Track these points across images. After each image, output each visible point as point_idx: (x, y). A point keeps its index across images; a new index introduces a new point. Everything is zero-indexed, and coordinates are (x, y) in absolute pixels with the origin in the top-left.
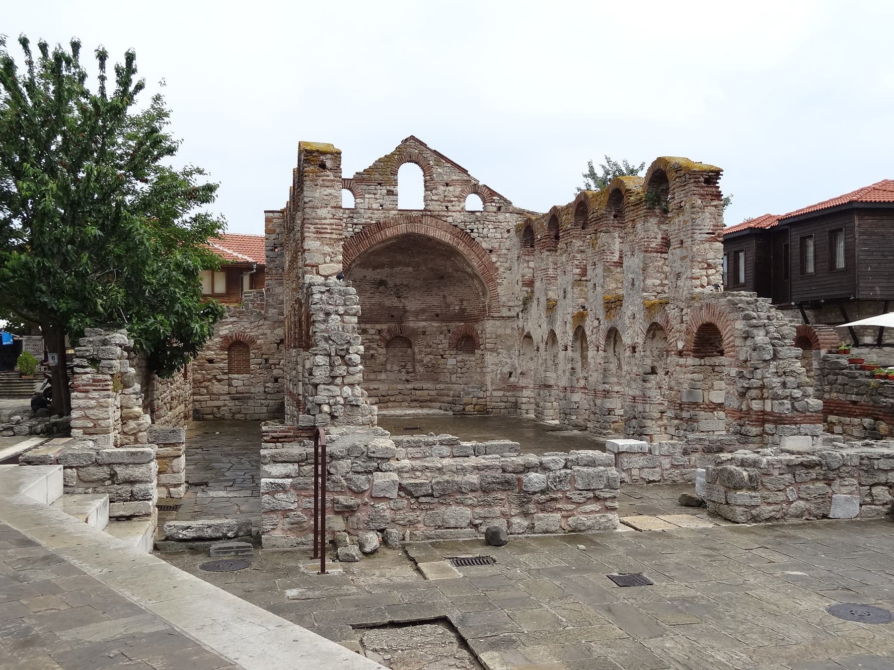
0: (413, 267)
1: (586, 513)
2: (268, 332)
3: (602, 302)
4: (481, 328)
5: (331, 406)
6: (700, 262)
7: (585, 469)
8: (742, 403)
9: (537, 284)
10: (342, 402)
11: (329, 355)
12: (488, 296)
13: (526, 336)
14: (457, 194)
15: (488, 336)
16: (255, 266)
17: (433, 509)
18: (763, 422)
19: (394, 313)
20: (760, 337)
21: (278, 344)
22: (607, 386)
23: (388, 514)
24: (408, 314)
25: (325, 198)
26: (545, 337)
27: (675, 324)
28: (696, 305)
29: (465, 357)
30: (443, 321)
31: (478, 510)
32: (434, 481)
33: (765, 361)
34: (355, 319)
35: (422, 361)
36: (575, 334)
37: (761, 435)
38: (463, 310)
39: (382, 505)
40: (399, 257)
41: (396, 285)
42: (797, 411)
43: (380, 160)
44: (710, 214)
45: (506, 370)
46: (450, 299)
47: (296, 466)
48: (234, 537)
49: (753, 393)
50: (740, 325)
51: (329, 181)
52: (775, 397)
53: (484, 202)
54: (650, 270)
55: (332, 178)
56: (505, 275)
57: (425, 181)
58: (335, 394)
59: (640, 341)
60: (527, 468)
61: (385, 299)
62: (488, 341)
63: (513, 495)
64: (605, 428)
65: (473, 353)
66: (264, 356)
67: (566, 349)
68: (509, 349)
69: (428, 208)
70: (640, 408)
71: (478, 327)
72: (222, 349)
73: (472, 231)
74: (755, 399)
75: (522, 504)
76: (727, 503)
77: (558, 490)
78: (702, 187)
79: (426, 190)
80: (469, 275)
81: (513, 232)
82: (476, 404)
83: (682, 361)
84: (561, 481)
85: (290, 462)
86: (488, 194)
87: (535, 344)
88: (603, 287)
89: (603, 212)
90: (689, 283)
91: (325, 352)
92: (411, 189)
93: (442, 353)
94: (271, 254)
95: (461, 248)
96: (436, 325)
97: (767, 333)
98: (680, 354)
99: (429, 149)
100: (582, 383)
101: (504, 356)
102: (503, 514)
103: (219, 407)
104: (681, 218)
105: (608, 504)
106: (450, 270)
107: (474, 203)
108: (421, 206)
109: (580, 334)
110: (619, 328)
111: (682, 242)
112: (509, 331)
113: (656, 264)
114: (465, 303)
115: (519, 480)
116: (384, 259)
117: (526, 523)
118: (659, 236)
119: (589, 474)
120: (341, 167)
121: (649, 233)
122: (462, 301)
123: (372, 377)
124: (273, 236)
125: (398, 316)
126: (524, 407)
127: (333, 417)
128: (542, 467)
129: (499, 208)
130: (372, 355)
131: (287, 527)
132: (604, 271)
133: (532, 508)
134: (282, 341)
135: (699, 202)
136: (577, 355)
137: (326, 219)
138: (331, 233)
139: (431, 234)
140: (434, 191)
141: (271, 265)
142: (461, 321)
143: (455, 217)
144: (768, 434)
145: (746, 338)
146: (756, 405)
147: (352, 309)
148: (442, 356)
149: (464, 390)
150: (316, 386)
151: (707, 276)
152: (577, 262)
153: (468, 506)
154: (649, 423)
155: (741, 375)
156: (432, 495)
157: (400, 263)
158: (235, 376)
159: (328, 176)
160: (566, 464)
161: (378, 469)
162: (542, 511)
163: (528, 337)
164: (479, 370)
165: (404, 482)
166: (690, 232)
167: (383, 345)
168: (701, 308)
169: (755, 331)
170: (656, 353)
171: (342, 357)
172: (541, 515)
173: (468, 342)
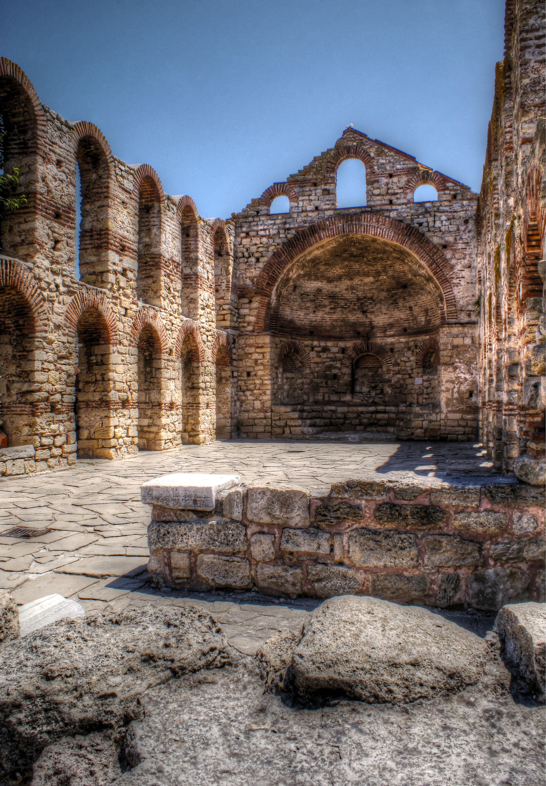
0: (374, 277)
19: (361, 329)
24: (375, 330)
30: (410, 335)
35: (389, 381)
38: (428, 322)
40: (356, 266)
41: (359, 299)
43: (315, 159)
45: (464, 388)
46: (416, 310)
56: (464, 273)
57: (367, 175)
61: (349, 315)
79: (368, 184)
92: (351, 186)
93: (410, 372)
96: (403, 340)
99: (369, 139)
106: (410, 276)
112: (468, 341)
116: (337, 271)
122: (426, 311)
123: (334, 398)
125: (365, 333)
129: (455, 197)
140: (376, 185)
157: (358, 273)
167: (348, 363)
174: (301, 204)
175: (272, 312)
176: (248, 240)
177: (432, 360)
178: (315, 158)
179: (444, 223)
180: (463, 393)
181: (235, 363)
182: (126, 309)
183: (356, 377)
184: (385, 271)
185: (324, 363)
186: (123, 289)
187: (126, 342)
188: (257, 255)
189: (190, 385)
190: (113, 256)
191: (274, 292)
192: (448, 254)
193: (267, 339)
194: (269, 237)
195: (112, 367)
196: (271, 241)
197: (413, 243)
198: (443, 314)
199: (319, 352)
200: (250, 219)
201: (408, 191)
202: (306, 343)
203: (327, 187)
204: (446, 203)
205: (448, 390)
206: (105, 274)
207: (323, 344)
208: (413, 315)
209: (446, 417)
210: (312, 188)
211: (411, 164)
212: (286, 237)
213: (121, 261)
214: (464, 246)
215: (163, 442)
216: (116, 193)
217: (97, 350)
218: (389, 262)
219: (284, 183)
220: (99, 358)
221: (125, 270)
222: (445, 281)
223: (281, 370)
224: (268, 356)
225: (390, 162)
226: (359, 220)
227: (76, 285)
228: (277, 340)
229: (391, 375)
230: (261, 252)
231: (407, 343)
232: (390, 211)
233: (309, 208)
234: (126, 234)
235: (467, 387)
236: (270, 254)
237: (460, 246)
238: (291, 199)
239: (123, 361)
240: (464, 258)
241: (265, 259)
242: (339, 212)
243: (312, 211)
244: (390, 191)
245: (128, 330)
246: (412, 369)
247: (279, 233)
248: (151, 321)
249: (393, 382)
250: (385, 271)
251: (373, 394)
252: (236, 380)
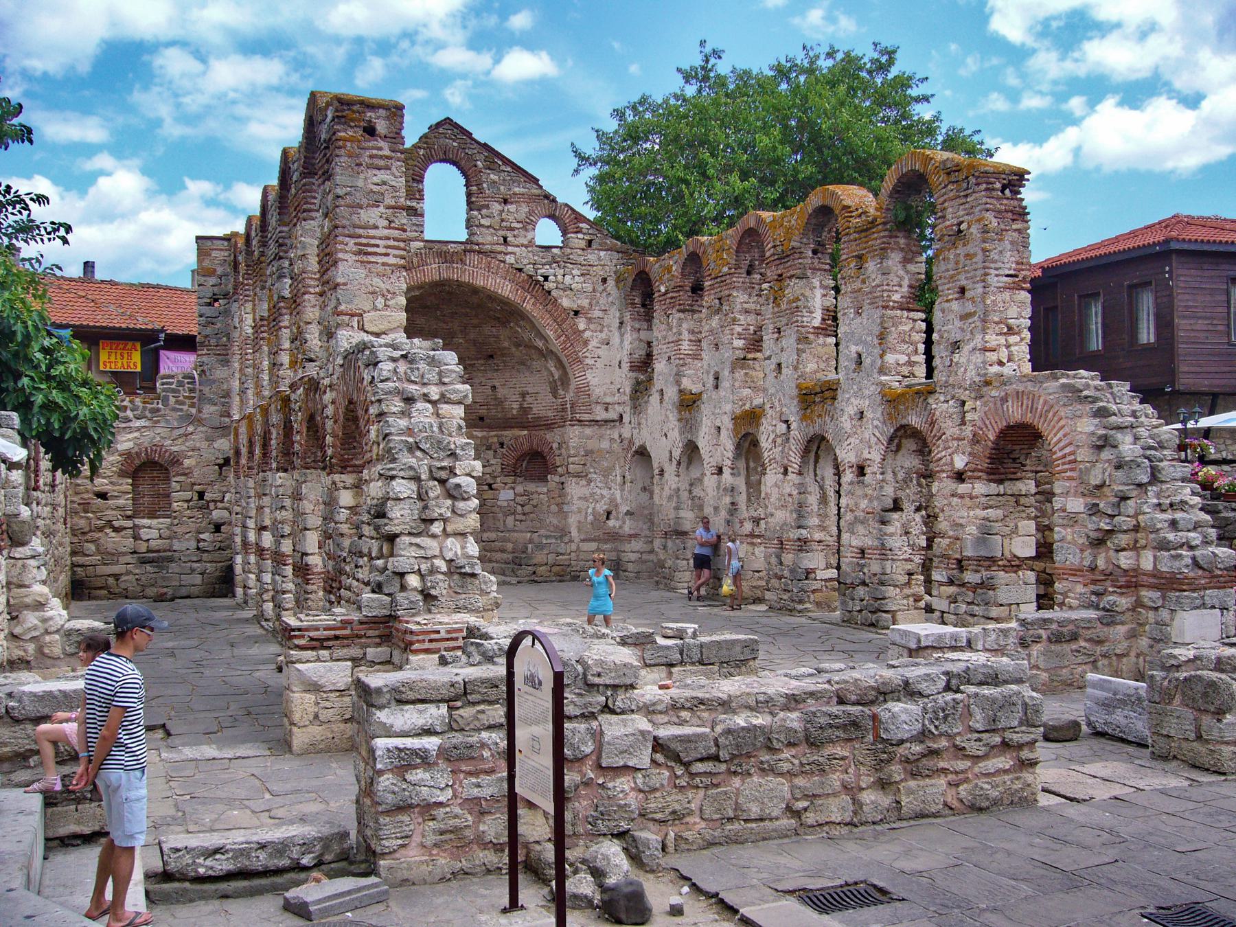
1: (988, 775)
2: (204, 445)
3: (795, 392)
4: (558, 439)
5: (422, 576)
6: (996, 323)
7: (986, 691)
8: (1095, 558)
9: (660, 366)
10: (444, 568)
11: (417, 479)
12: (572, 387)
13: (636, 452)
14: (522, 216)
16: (162, 336)
17: (717, 786)
18: (1137, 586)
20: (1127, 447)
21: (221, 466)
22: (804, 532)
23: (633, 800)
25: (375, 188)
26: (677, 454)
27: (950, 428)
28: (994, 393)
29: (531, 487)
30: (491, 428)
31: (800, 781)
32: (719, 729)
33: (1140, 485)
34: (460, 411)
36: (738, 447)
37: (1133, 610)
39: (623, 784)
42: (1201, 568)
44: (1012, 243)
45: (601, 507)
46: (501, 392)
47: (444, 709)
48: (315, 866)
49: (1123, 539)
50: (1087, 426)
51: (381, 157)
52: (1164, 546)
53: (564, 233)
54: (892, 338)
55: (387, 152)
56: (600, 352)
57: (469, 195)
58: (430, 553)
59: (876, 456)
60: (884, 693)
62: (571, 460)
63: (860, 750)
64: (801, 602)
66: (196, 488)
67: (720, 471)
69: (474, 239)
70: (875, 567)
71: (553, 437)
72: (122, 474)
73: (546, 278)
74: (1123, 550)
75: (880, 765)
76: (1199, 737)
77: (941, 735)
78: (998, 199)
80: (540, 351)
81: (611, 283)
82: (554, 565)
83: (963, 488)
84: (946, 717)
85: (431, 702)
86: (567, 219)
87: (655, 465)
88: (796, 368)
89: (793, 244)
90: (978, 358)
91: (411, 473)
94: (208, 311)
95: (528, 306)
97: (1136, 438)
98: (960, 477)
100: (748, 527)
101: (598, 487)
102: (846, 788)
103: (117, 577)
104: (961, 250)
105: (1025, 754)
106: (506, 344)
108: (463, 236)
109: (747, 446)
110: (829, 437)
111: (962, 290)
112: (605, 445)
113: (901, 328)
114: (528, 398)
115: (874, 717)
117: (886, 801)
118: (906, 283)
119: (993, 701)
120: (403, 133)
121: (892, 276)
122: (524, 395)
124: (212, 280)
126: (630, 567)
127: (428, 597)
128: (908, 691)
129: (590, 243)
131: (431, 839)
132: (799, 341)
133: (896, 771)
134: (227, 461)
135: (994, 223)
136: (740, 483)
137: (376, 227)
138: (387, 255)
139: (480, 282)
140: (484, 211)
141: (208, 331)
142: (523, 428)
143: (515, 255)
144: (1144, 606)
145: (1100, 448)
146: (1125, 560)
147: (456, 391)
148: (490, 485)
149: (531, 541)
150: (392, 538)
151: (1008, 346)
152: (739, 329)
153: (781, 775)
154: (891, 592)
155: (1094, 510)
156: (716, 758)
158: (146, 522)
159: (380, 149)
160: (948, 682)
161: (607, 709)
162: (913, 775)
163: (642, 454)
164: (554, 508)
165: (664, 733)
166: (980, 272)
168: (1004, 400)
169: (1119, 436)
170: (901, 475)
171: (442, 482)
172: (912, 784)
184: (464, 331)
192: (581, 324)
203: (414, 204)
204: (580, 252)
208: (496, 399)
209: (578, 547)
214: (600, 314)
218: (475, 321)
226: (463, 262)
231: (487, 438)
232: (506, 254)
240: (601, 331)
244: (504, 224)
250: (464, 331)
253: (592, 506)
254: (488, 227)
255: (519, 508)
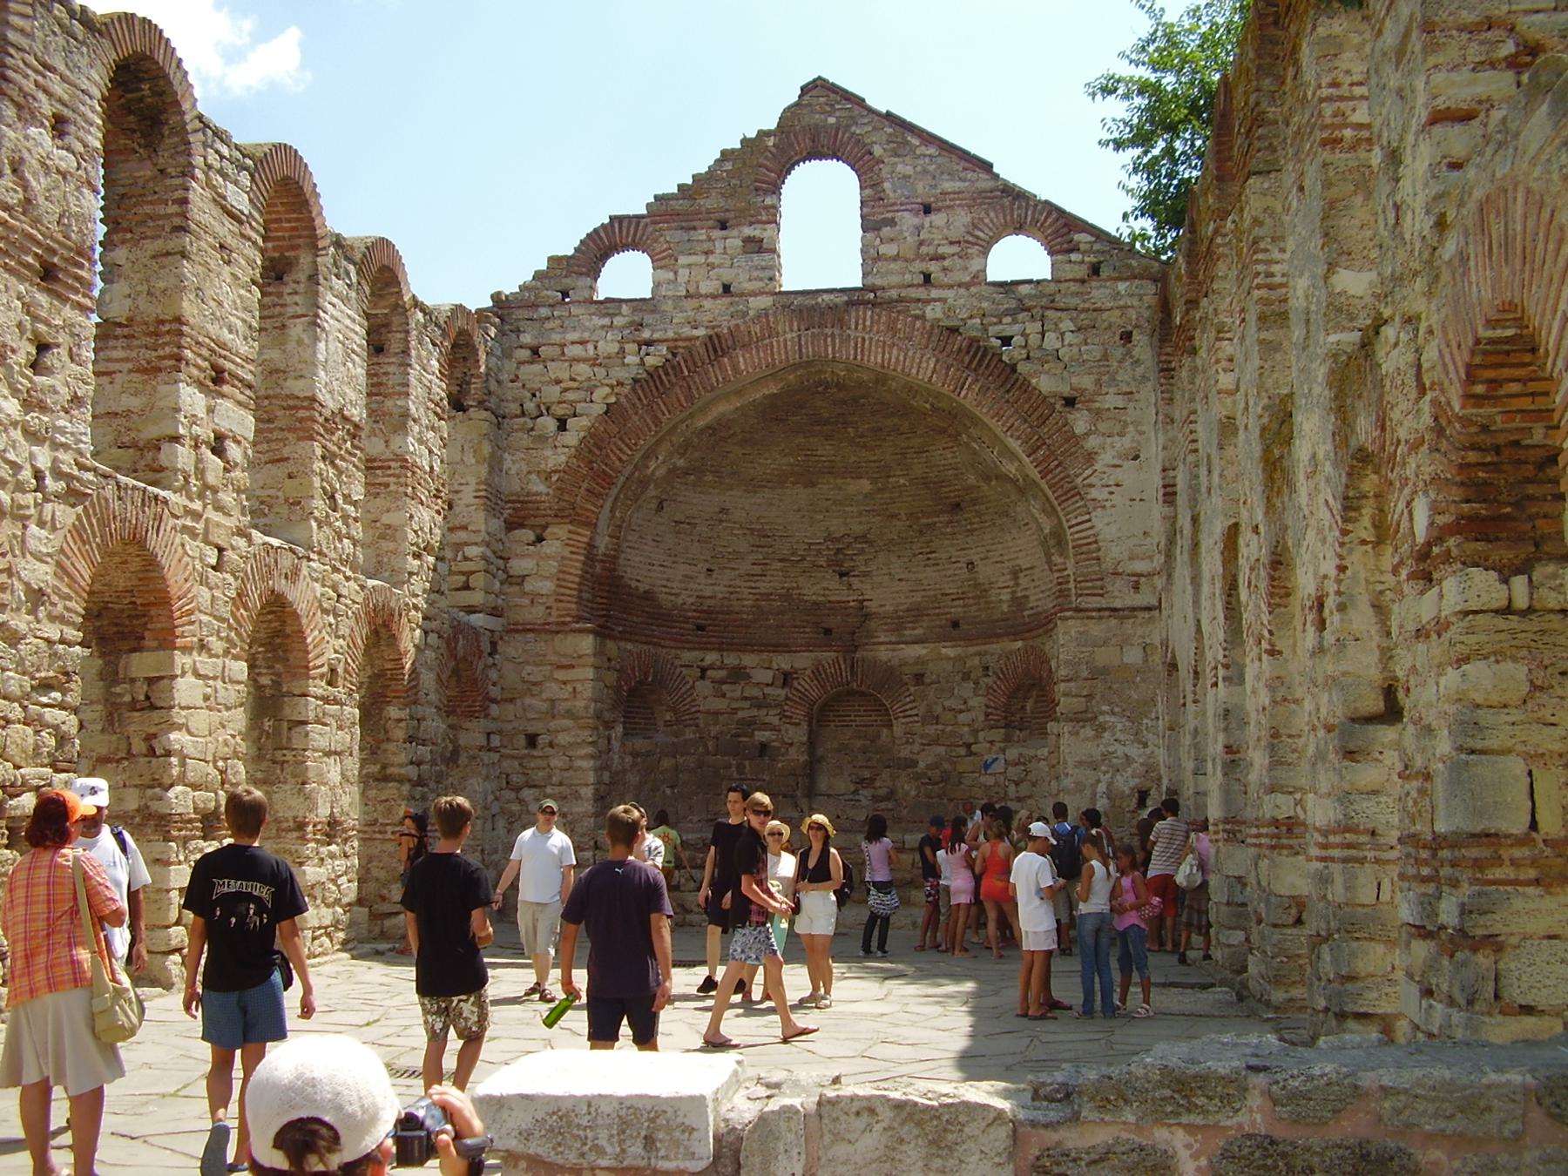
0: (874, 481)
14: (957, 231)
15: (1063, 672)
19: (833, 622)
24: (873, 624)
30: (969, 639)
35: (914, 764)
38: (1019, 602)
41: (829, 538)
46: (985, 572)
56: (1118, 475)
65: (1044, 733)
68: (1136, 714)
80: (1014, 481)
92: (820, 233)
96: (951, 652)
99: (870, 110)
106: (972, 479)
107: (1019, 259)
108: (857, 282)
112: (1133, 656)
114: (1023, 581)
122: (1015, 573)
125: (843, 630)
129: (1095, 270)
130: (764, 748)
139: (875, 358)
140: (886, 231)
163: (1173, 667)
167: (799, 713)
173: (1026, 701)
174: (683, 274)
175: (598, 569)
176: (538, 367)
177: (1029, 705)
178: (724, 153)
179: (1069, 337)
180: (1122, 796)
181: (494, 710)
182: (221, 550)
183: (820, 751)
185: (735, 711)
186: (215, 491)
187: (217, 645)
188: (560, 410)
189: (375, 769)
190: (191, 398)
191: (605, 513)
192: (1080, 422)
193: (587, 644)
194: (594, 362)
195: (178, 716)
196: (601, 372)
197: (984, 390)
198: (1062, 582)
199: (722, 682)
200: (544, 312)
201: (974, 250)
202: (688, 656)
204: (1074, 287)
205: (1080, 787)
206: (165, 447)
207: (731, 659)
208: (976, 585)
210: (717, 233)
211: (984, 183)
212: (642, 363)
213: (211, 410)
215: (308, 934)
216: (206, 219)
217: (141, 664)
219: (642, 217)
220: (141, 690)
221: (220, 438)
222: (1072, 493)
223: (619, 729)
224: (587, 690)
225: (925, 171)
226: (842, 323)
227: (90, 476)
228: (610, 644)
229: (916, 747)
230: (571, 403)
232: (928, 302)
233: (705, 287)
234: (227, 336)
235: (1132, 783)
236: (599, 409)
237: (1111, 400)
238: (657, 263)
239: (206, 698)
240: (1121, 434)
241: (585, 422)
242: (784, 299)
243: (714, 297)
244: (924, 250)
245: (225, 611)
246: (975, 732)
247: (622, 350)
248: (281, 585)
249: (921, 765)
251: (865, 794)
252: (495, 757)
253: (1105, 778)
254: (895, 258)
255: (1012, 788)
